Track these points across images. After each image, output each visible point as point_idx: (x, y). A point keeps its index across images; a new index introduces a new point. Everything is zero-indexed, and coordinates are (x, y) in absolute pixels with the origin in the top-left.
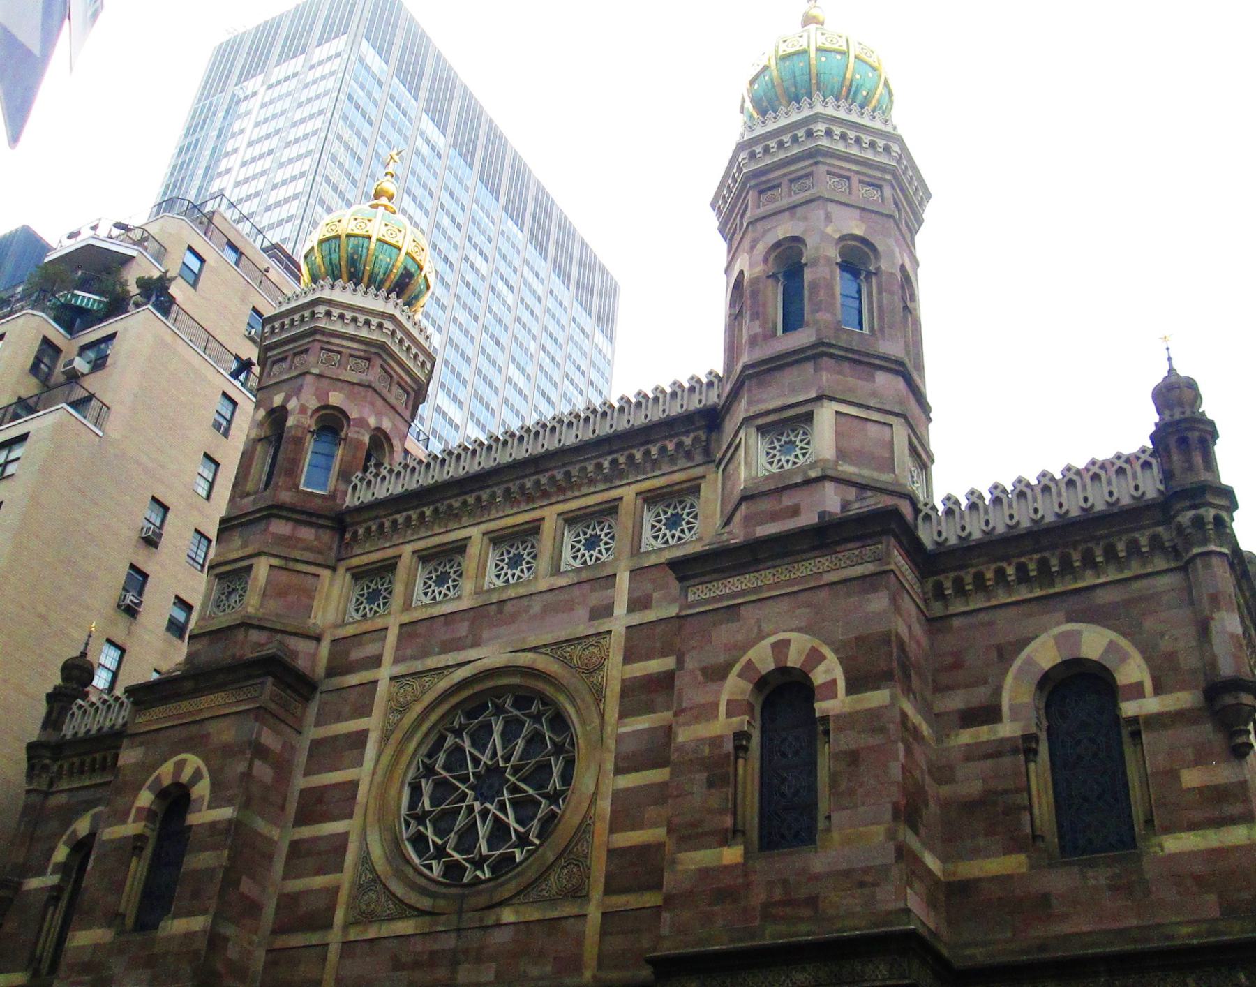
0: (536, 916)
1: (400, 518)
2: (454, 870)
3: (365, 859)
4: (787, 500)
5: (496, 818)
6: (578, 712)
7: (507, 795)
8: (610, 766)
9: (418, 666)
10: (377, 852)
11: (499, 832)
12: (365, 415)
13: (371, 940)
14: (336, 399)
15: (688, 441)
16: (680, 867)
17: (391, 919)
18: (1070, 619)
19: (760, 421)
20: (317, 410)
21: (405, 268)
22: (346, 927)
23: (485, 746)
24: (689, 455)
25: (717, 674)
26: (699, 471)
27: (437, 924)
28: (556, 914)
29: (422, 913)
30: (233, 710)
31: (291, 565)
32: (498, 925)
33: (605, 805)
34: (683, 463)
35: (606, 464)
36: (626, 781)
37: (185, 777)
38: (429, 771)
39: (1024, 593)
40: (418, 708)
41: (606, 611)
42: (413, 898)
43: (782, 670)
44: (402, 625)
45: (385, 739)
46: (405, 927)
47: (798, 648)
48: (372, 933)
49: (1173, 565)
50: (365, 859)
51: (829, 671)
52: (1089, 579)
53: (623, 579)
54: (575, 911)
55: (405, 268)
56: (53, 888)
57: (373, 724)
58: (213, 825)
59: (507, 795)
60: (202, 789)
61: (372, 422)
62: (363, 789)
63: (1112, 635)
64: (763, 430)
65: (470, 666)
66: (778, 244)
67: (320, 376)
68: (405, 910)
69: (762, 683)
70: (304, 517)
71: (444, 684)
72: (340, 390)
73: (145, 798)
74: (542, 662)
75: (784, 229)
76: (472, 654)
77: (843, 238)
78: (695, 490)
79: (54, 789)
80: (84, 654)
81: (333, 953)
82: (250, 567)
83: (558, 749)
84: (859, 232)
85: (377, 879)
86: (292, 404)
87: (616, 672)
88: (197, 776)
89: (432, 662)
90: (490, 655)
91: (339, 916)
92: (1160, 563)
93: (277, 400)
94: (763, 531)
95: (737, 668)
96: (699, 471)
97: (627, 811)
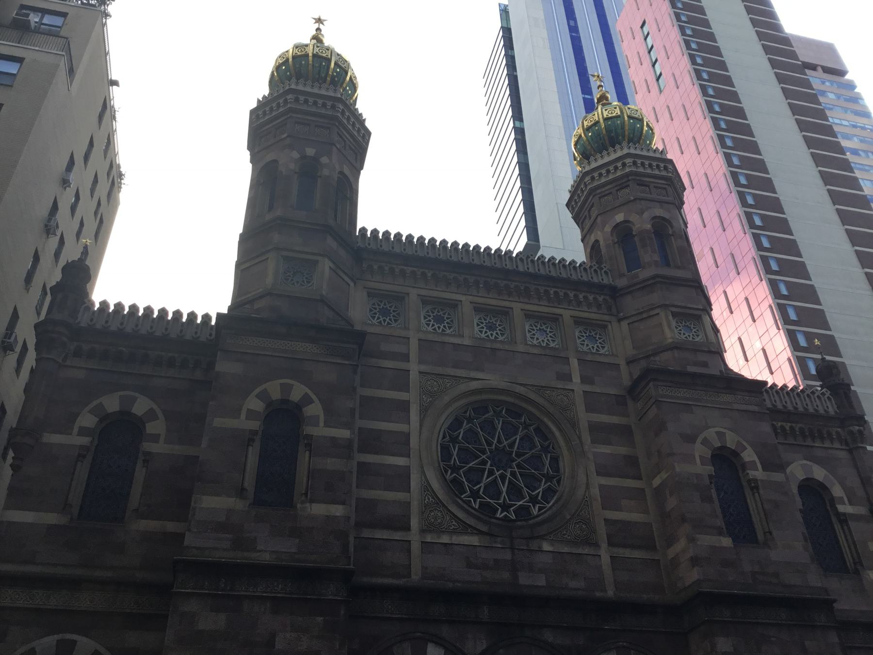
0: (566, 550)
1: (409, 269)
3: (427, 487)
4: (702, 357)
5: (495, 480)
6: (560, 430)
8: (592, 468)
9: (439, 370)
10: (436, 484)
11: (515, 491)
13: (445, 544)
15: (601, 299)
16: (699, 543)
17: (454, 532)
18: (805, 459)
19: (674, 309)
23: (494, 435)
24: (599, 306)
25: (690, 439)
26: (606, 318)
27: (496, 542)
28: (580, 551)
29: (480, 532)
30: (330, 360)
33: (595, 491)
34: (594, 309)
35: (552, 292)
36: (604, 481)
37: (296, 396)
38: (454, 440)
39: (791, 441)
40: (447, 399)
41: (568, 378)
42: (471, 521)
43: (723, 448)
44: (419, 340)
45: (424, 411)
46: (474, 540)
47: (731, 440)
48: (445, 539)
49: (844, 447)
50: (427, 487)
51: (749, 455)
52: (809, 442)
53: (574, 363)
54: (592, 551)
56: (81, 447)
57: (412, 396)
58: (333, 439)
60: (315, 409)
62: (414, 442)
63: (825, 472)
64: (674, 315)
65: (476, 382)
66: (655, 218)
68: (466, 529)
69: (736, 454)
71: (463, 387)
73: (255, 404)
74: (532, 396)
75: (659, 212)
76: (480, 375)
78: (605, 327)
79: (68, 363)
81: (416, 547)
82: (317, 261)
83: (545, 449)
85: (439, 502)
86: (324, 160)
87: (584, 417)
88: (306, 400)
89: (473, 374)
90: (491, 378)
91: (414, 523)
92: (837, 445)
93: (310, 152)
94: (691, 369)
95: (699, 440)
96: (606, 318)
97: (610, 499)
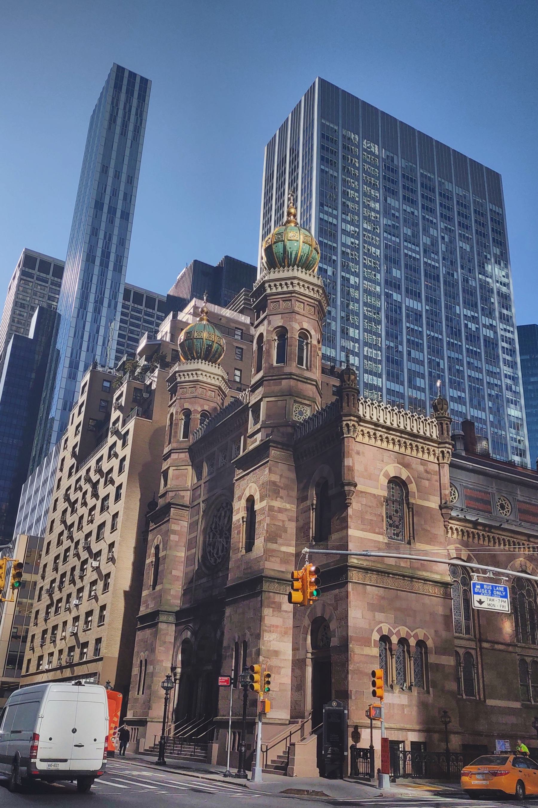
2: (216, 560)
7: (224, 536)
12: (196, 408)
14: (186, 406)
20: (182, 411)
21: (207, 345)
22: (196, 581)
31: (179, 468)
32: (219, 577)
55: (207, 345)
59: (224, 536)
61: (199, 409)
67: (180, 399)
70: (181, 451)
72: (188, 402)
77: (275, 329)
80: (154, 499)
84: (280, 324)
